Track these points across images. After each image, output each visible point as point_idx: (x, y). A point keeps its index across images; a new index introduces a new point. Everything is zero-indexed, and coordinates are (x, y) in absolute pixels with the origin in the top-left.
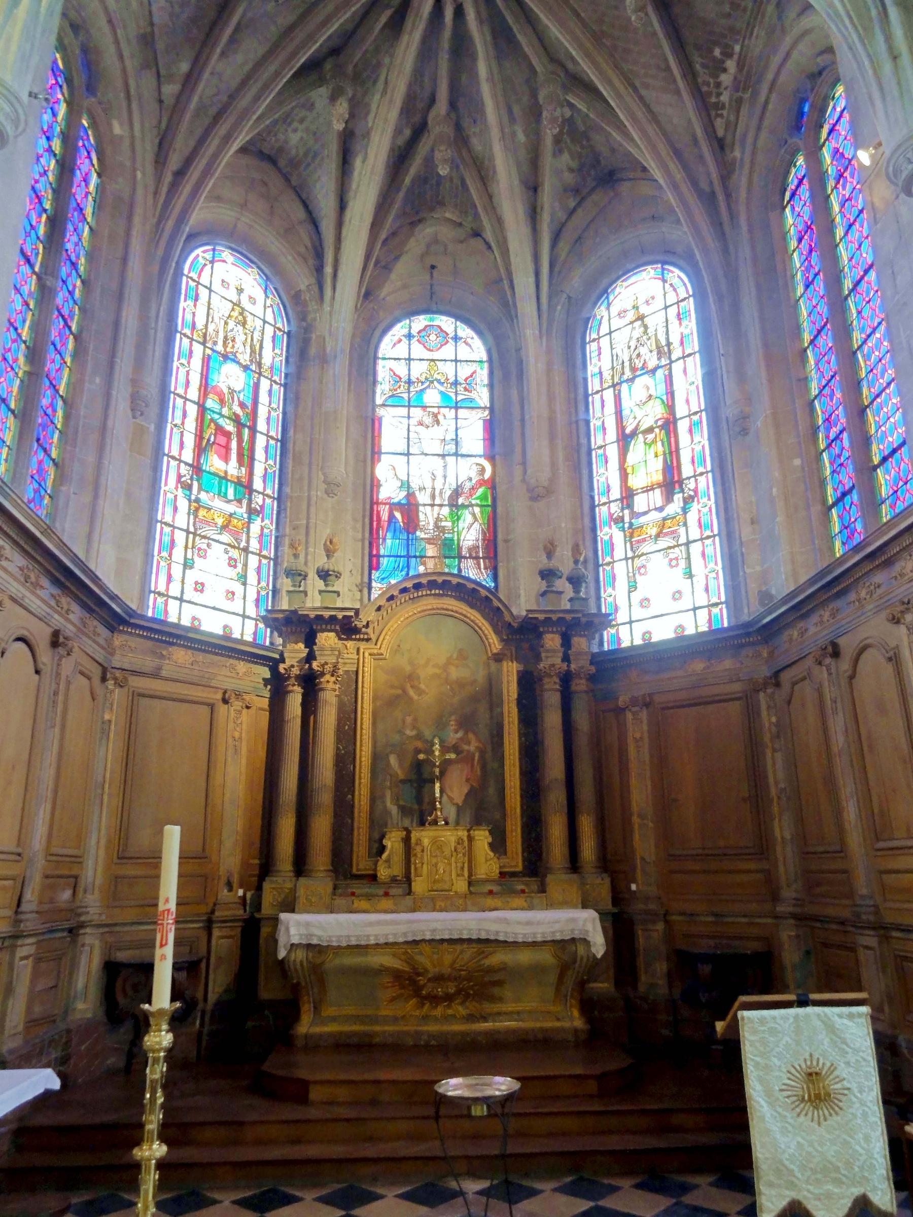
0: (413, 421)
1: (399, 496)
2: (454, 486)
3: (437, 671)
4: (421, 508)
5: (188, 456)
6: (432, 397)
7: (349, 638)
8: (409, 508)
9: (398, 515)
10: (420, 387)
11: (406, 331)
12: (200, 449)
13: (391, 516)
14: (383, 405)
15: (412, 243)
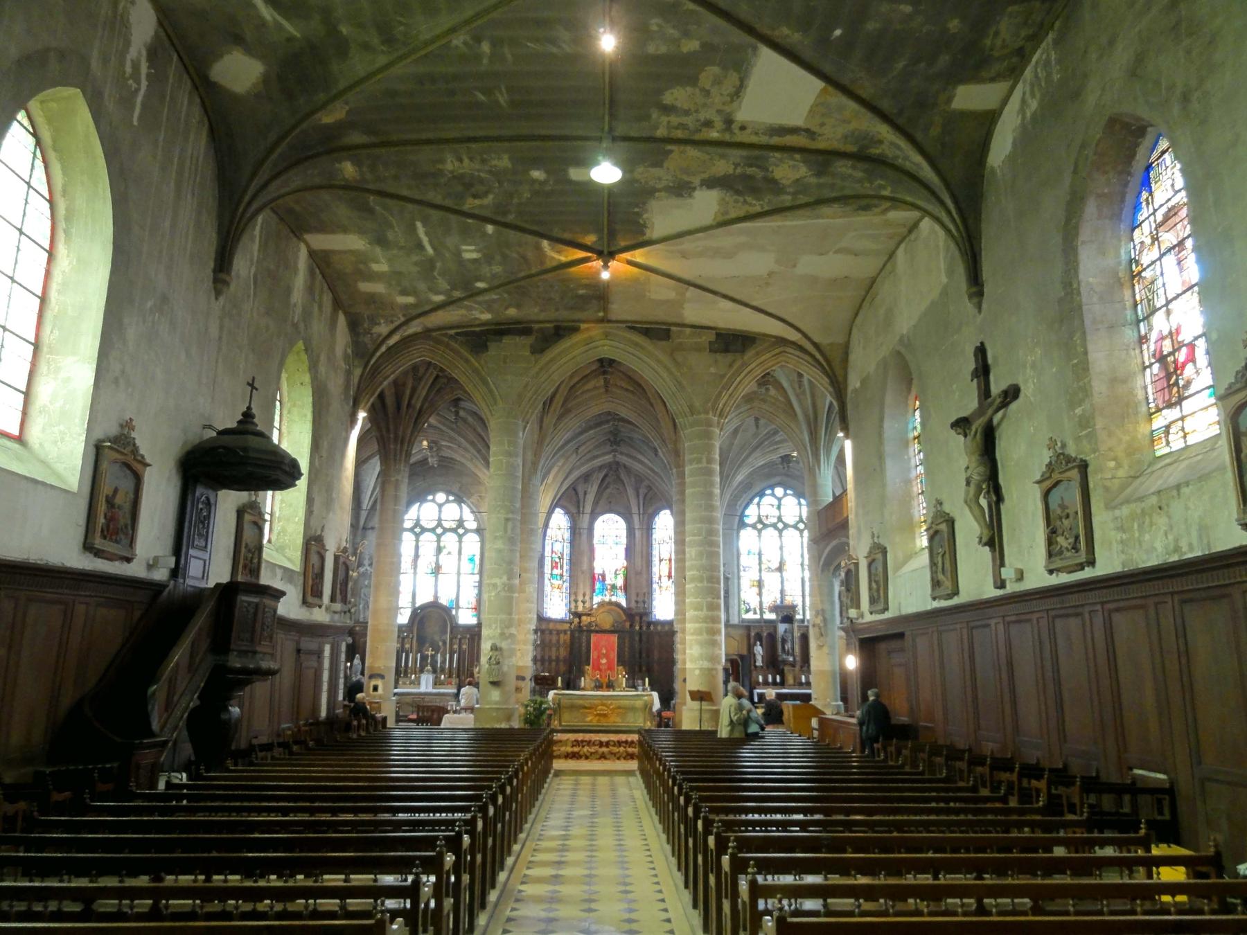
8: (603, 576)
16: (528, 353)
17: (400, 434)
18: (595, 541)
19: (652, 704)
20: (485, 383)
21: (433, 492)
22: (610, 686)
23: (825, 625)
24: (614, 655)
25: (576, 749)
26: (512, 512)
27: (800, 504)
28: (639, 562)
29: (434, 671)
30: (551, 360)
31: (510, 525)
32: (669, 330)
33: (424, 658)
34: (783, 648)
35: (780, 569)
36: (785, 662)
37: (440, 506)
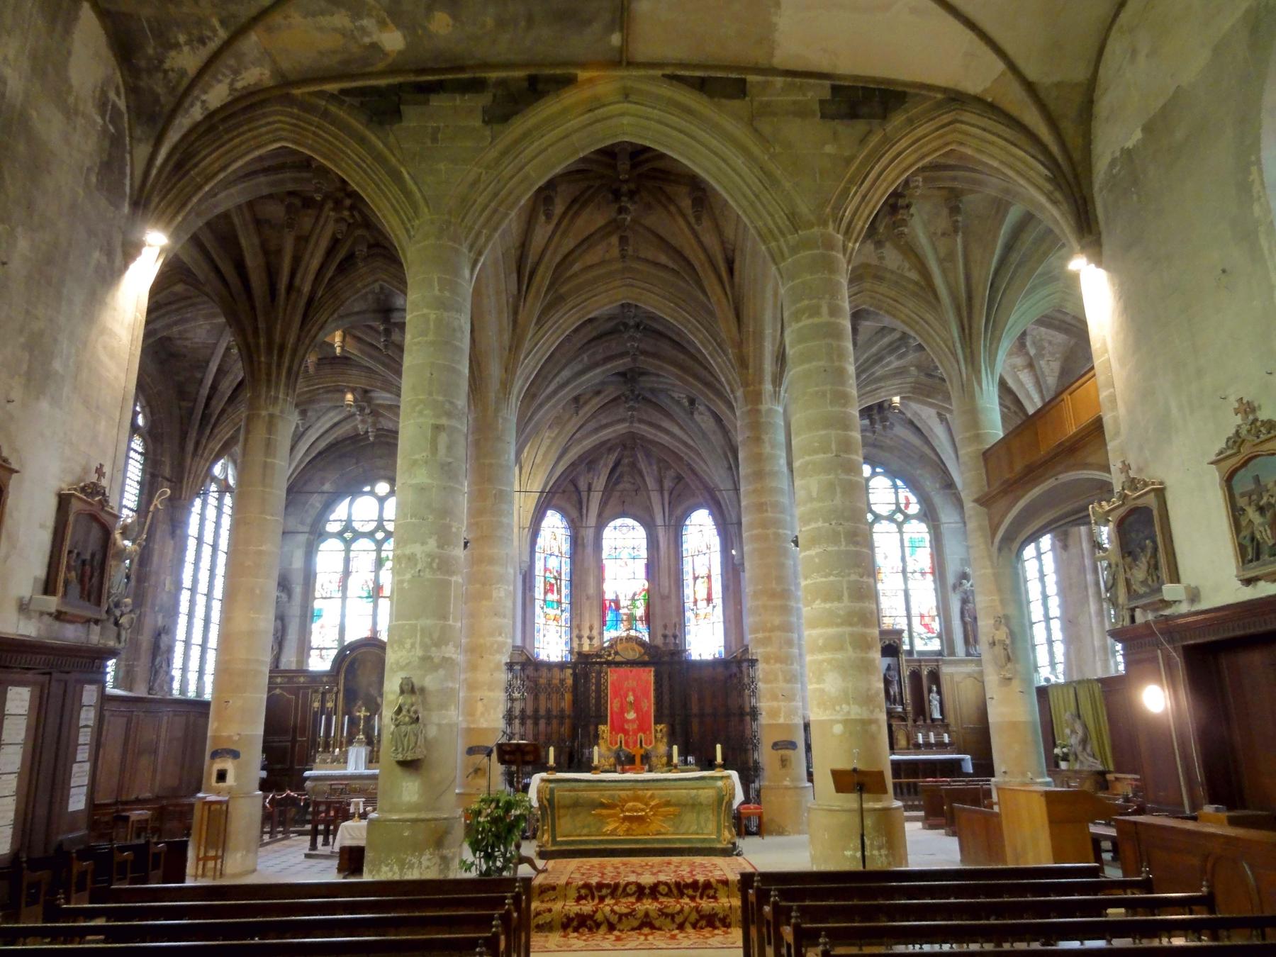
1: (613, 597)
5: (542, 597)
8: (617, 602)
12: (546, 593)
16: (478, 123)
17: (277, 339)
18: (604, 555)
19: (733, 796)
20: (397, 177)
21: (372, 481)
22: (646, 760)
23: (1013, 642)
24: (649, 705)
25: (587, 907)
26: (449, 415)
27: (895, 487)
28: (665, 582)
29: (369, 742)
30: (526, 135)
31: (443, 438)
32: (744, 81)
33: (353, 722)
37: (382, 500)
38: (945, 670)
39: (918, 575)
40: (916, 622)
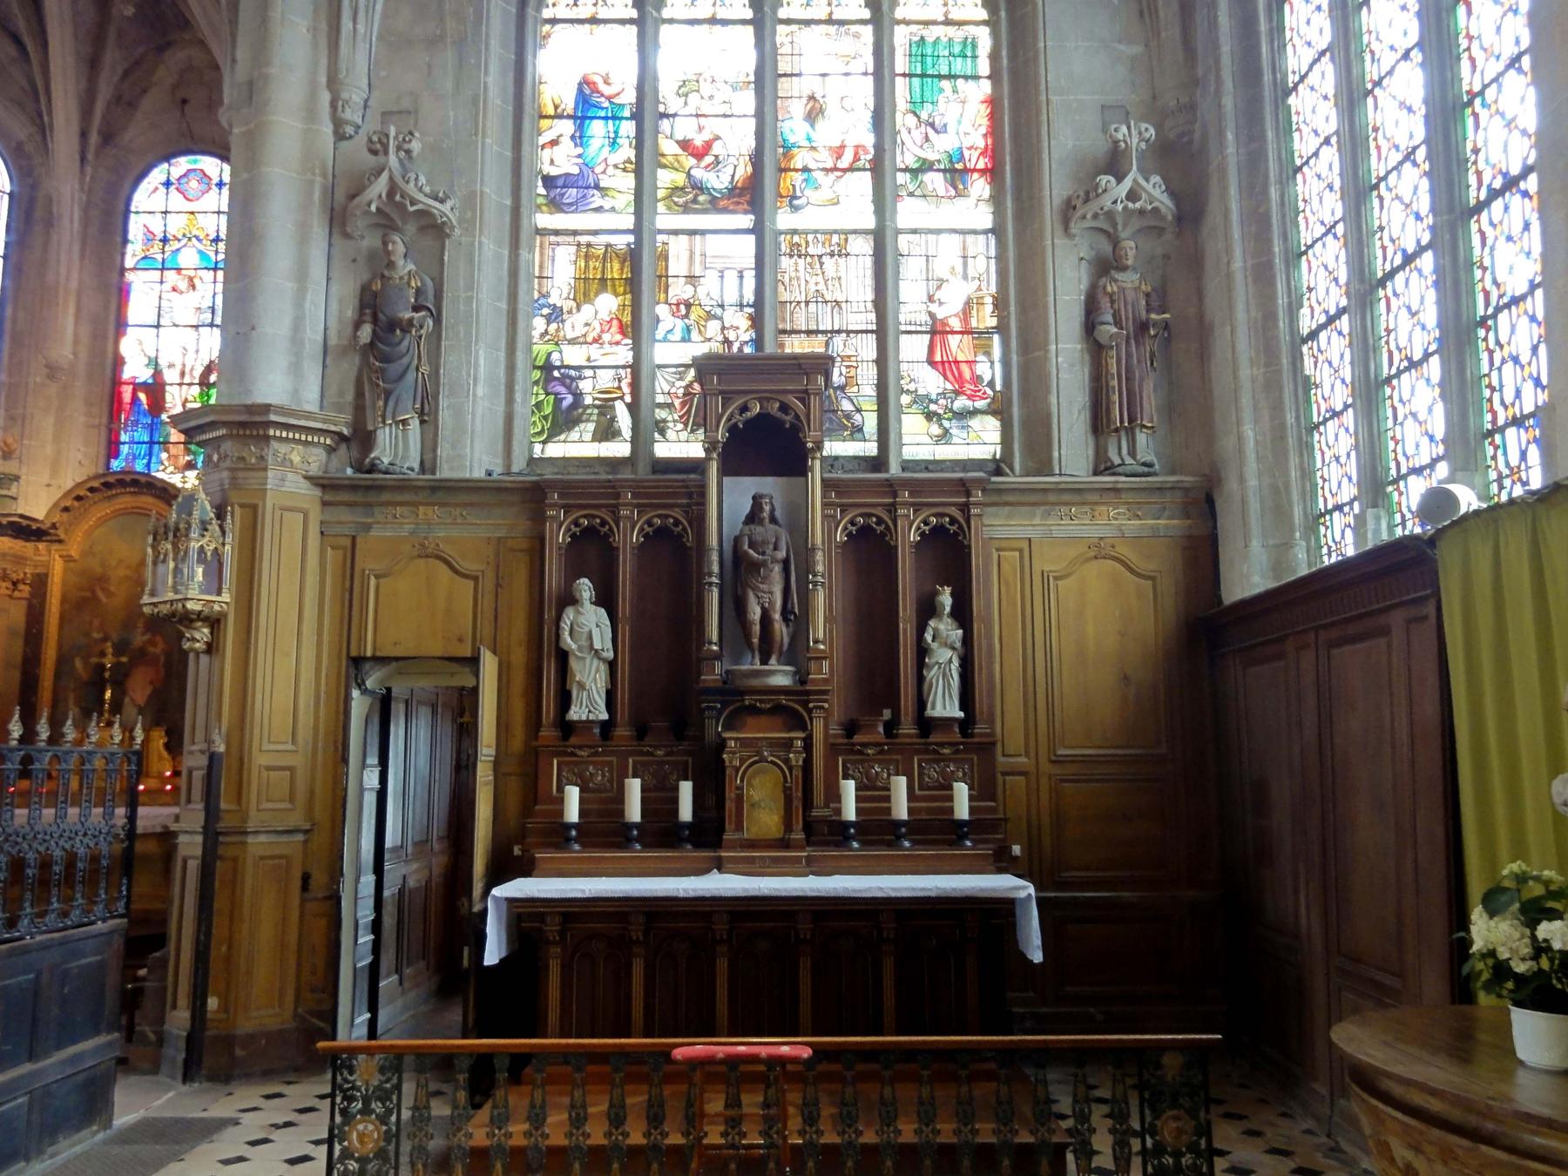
0: (167, 287)
1: (145, 375)
2: (206, 362)
3: (128, 573)
4: (168, 388)
6: (188, 258)
7: (39, 540)
8: (155, 390)
9: (142, 396)
10: (176, 245)
11: (163, 178)
13: (135, 399)
14: (135, 269)
15: (161, 72)
34: (735, 606)
35: (751, 194)
36: (740, 701)
38: (997, 530)
39: (935, 181)
40: (912, 349)
